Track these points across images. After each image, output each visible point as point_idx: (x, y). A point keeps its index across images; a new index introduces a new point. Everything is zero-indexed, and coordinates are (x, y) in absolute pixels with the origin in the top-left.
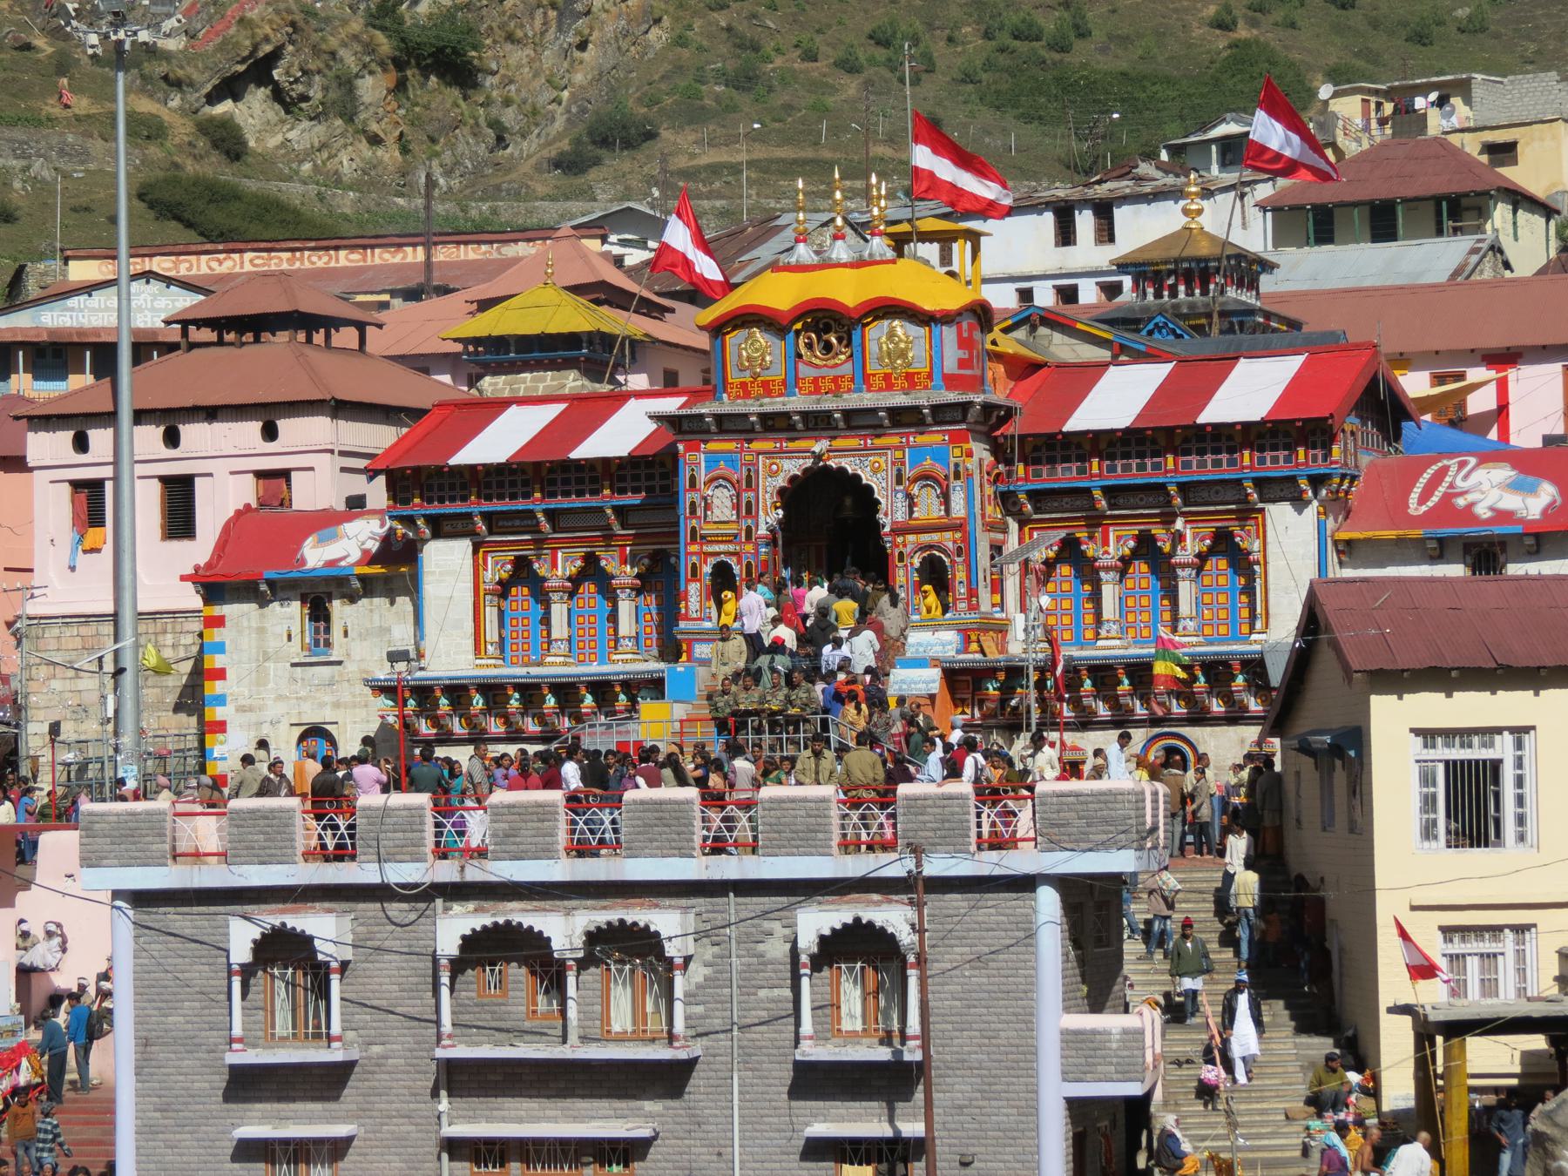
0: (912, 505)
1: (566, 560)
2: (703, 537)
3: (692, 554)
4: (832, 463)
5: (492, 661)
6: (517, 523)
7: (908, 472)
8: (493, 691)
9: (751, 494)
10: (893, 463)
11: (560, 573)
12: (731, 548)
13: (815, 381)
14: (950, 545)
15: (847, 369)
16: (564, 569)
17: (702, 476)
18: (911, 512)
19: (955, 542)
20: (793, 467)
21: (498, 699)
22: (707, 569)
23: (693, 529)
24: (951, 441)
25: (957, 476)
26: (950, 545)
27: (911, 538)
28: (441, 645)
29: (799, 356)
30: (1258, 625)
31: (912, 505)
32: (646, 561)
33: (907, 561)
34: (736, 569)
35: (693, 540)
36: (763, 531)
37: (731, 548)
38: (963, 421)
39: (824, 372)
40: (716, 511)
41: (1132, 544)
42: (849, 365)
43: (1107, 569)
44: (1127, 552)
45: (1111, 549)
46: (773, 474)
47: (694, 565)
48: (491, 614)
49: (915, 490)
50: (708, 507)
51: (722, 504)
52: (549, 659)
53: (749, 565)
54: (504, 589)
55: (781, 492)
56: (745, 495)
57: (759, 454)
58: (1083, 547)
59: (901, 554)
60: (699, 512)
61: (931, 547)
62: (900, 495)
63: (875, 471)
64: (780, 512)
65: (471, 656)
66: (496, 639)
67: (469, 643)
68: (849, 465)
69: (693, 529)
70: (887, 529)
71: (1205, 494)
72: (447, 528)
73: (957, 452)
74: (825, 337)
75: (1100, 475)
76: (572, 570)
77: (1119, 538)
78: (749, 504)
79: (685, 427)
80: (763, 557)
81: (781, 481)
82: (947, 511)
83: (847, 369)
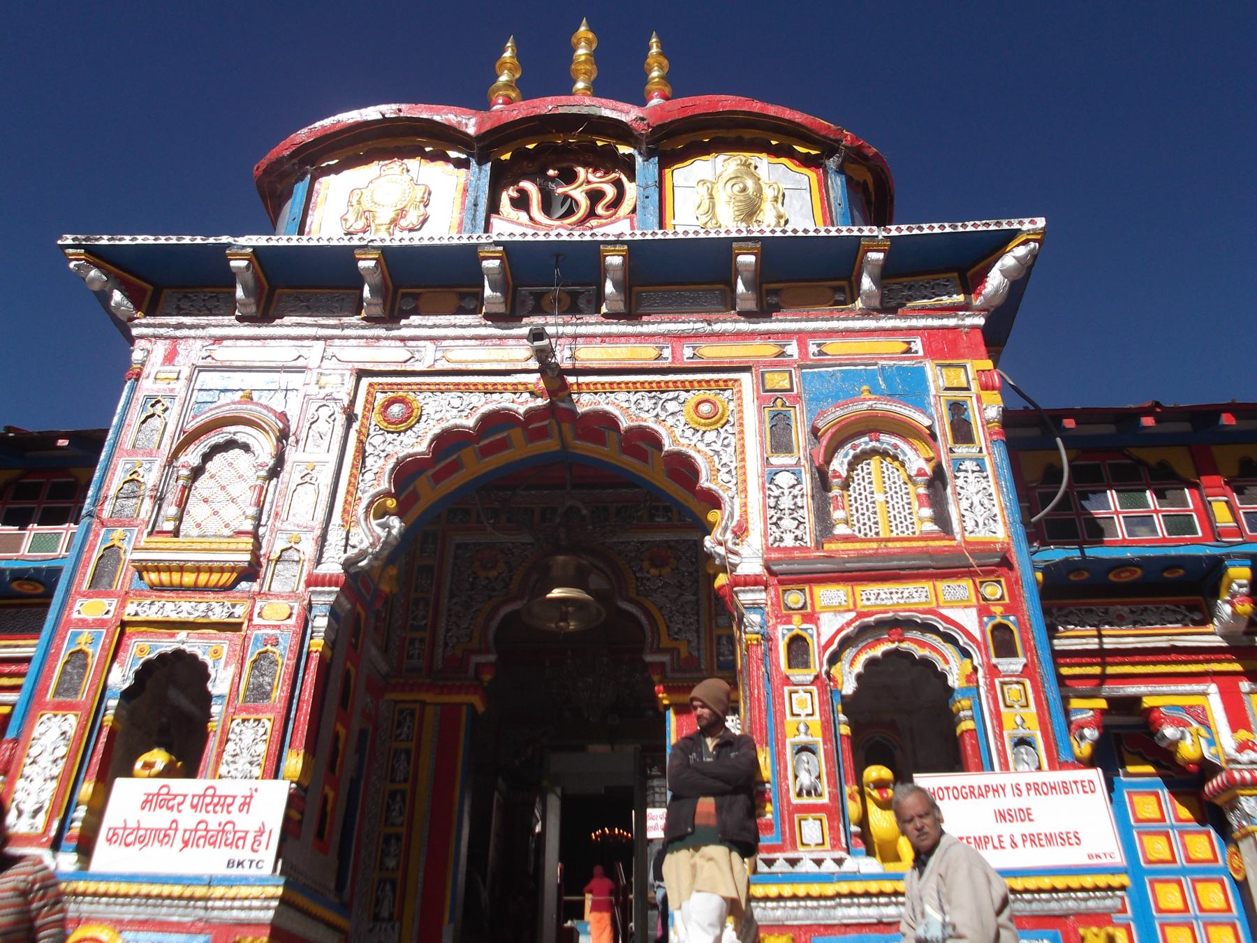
2: (142, 569)
3: (84, 623)
12: (218, 614)
14: (969, 619)
19: (984, 611)
20: (447, 411)
22: (121, 677)
24: (930, 353)
26: (969, 619)
33: (817, 664)
35: (99, 585)
36: (332, 566)
38: (965, 307)
55: (406, 472)
61: (897, 625)
64: (396, 523)
68: (628, 408)
81: (416, 443)
82: (942, 519)
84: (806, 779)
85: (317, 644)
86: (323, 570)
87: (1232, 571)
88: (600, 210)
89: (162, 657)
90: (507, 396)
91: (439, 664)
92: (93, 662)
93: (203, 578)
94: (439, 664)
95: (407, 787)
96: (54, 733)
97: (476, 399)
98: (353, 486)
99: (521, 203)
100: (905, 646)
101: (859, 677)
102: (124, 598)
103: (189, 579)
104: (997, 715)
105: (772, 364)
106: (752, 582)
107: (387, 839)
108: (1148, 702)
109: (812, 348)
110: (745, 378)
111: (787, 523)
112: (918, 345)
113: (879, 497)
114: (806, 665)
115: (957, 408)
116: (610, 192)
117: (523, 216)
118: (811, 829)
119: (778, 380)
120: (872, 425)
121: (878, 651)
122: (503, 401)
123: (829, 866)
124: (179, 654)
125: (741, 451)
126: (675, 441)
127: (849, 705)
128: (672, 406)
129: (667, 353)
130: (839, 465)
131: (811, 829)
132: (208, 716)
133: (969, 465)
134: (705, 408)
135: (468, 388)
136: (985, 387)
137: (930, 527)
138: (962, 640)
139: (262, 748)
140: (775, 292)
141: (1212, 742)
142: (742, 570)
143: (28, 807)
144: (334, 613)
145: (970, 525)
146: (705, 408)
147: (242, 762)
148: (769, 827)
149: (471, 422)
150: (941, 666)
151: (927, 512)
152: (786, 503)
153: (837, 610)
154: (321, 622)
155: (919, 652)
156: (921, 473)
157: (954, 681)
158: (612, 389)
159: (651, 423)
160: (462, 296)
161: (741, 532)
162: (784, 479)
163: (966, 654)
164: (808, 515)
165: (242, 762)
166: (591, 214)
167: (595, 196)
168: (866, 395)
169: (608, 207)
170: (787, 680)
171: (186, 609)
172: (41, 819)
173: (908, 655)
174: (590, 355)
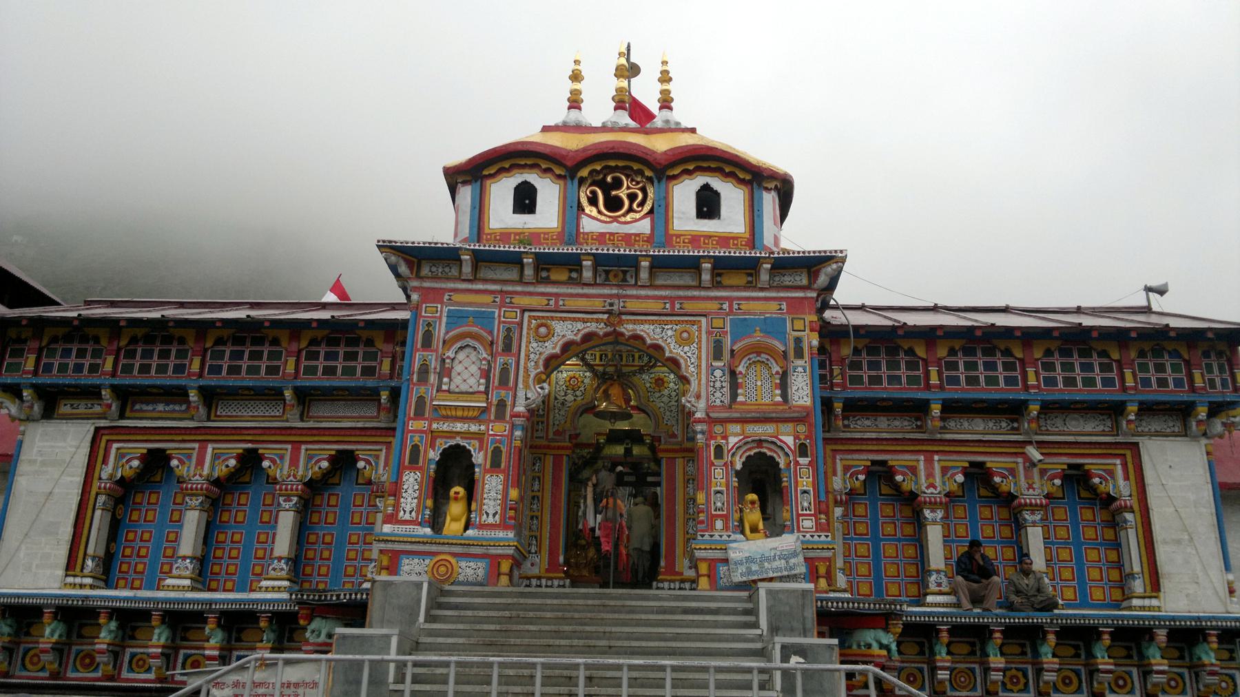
0: (734, 386)
1: (216, 457)
4: (628, 329)
5: (88, 581)
6: (160, 407)
7: (727, 342)
8: (76, 617)
9: (512, 360)
10: (709, 333)
11: (206, 472)
12: (474, 428)
13: (602, 235)
14: (790, 440)
15: (644, 226)
16: (212, 468)
17: (440, 332)
18: (734, 396)
21: (86, 631)
22: (434, 455)
23: (421, 401)
25: (799, 354)
26: (790, 440)
27: (737, 428)
28: (22, 555)
29: (580, 208)
30: (1138, 586)
31: (734, 386)
32: (325, 464)
33: (727, 458)
34: (478, 458)
35: (419, 414)
36: (520, 408)
37: (474, 428)
39: (614, 227)
40: (457, 380)
41: (960, 478)
42: (648, 220)
43: (933, 505)
44: (954, 487)
45: (938, 481)
46: (542, 339)
47: (415, 449)
48: (99, 520)
49: (741, 369)
50: (445, 372)
51: (467, 372)
52: (169, 581)
53: (497, 452)
54: (125, 493)
56: (500, 360)
57: (523, 311)
58: (899, 478)
59: (719, 449)
60: (433, 378)
61: (760, 442)
62: (718, 373)
63: (682, 342)
65: (60, 572)
66: (101, 553)
67: (61, 554)
68: (650, 332)
69: (421, 401)
70: (698, 415)
71: (1059, 422)
72: (64, 409)
73: (799, 325)
74: (614, 193)
75: (941, 387)
76: (221, 471)
77: (945, 470)
78: (505, 371)
79: (425, 271)
80: (518, 443)
82: (784, 395)
83: (644, 226)
84: (719, 504)
85: (518, 443)
86: (516, 409)
87: (933, 406)
88: (635, 206)
89: (451, 447)
90: (594, 324)
91: (551, 435)
92: (422, 449)
93: (466, 414)
94: (551, 435)
95: (540, 494)
96: (412, 480)
97: (580, 325)
98: (526, 370)
99: (593, 201)
100: (764, 450)
101: (744, 463)
102: (431, 421)
103: (460, 413)
104: (796, 482)
105: (717, 314)
106: (699, 421)
107: (532, 518)
108: (890, 463)
109: (736, 306)
110: (703, 320)
111: (718, 394)
112: (784, 307)
113: (759, 383)
114: (721, 458)
115: (798, 341)
116: (640, 196)
117: (594, 209)
118: (719, 524)
119: (718, 323)
120: (758, 349)
121: (752, 453)
122: (592, 327)
123: (725, 537)
124: (458, 446)
125: (699, 358)
126: (671, 352)
127: (738, 474)
128: (670, 333)
129: (668, 306)
130: (741, 369)
131: (719, 524)
132: (474, 473)
133: (800, 369)
134: (685, 335)
135: (574, 320)
136: (812, 330)
137: (779, 399)
138: (787, 450)
139: (500, 487)
140: (719, 275)
141: (916, 483)
142: (698, 415)
143: (408, 510)
144: (524, 429)
145: (796, 398)
146: (685, 335)
147: (493, 494)
148: (702, 522)
149: (578, 338)
150: (777, 459)
151: (778, 392)
152: (718, 384)
153: (736, 435)
154: (518, 433)
155: (769, 453)
156: (777, 373)
157: (782, 466)
158: (643, 322)
159: (660, 342)
160: (571, 270)
161: (698, 397)
162: (718, 373)
163: (787, 454)
164: (727, 390)
165: (493, 494)
166: (630, 210)
167: (632, 197)
168: (758, 334)
169: (638, 206)
170: (713, 464)
171: (459, 427)
172: (414, 514)
173: (764, 454)
174: (632, 305)
